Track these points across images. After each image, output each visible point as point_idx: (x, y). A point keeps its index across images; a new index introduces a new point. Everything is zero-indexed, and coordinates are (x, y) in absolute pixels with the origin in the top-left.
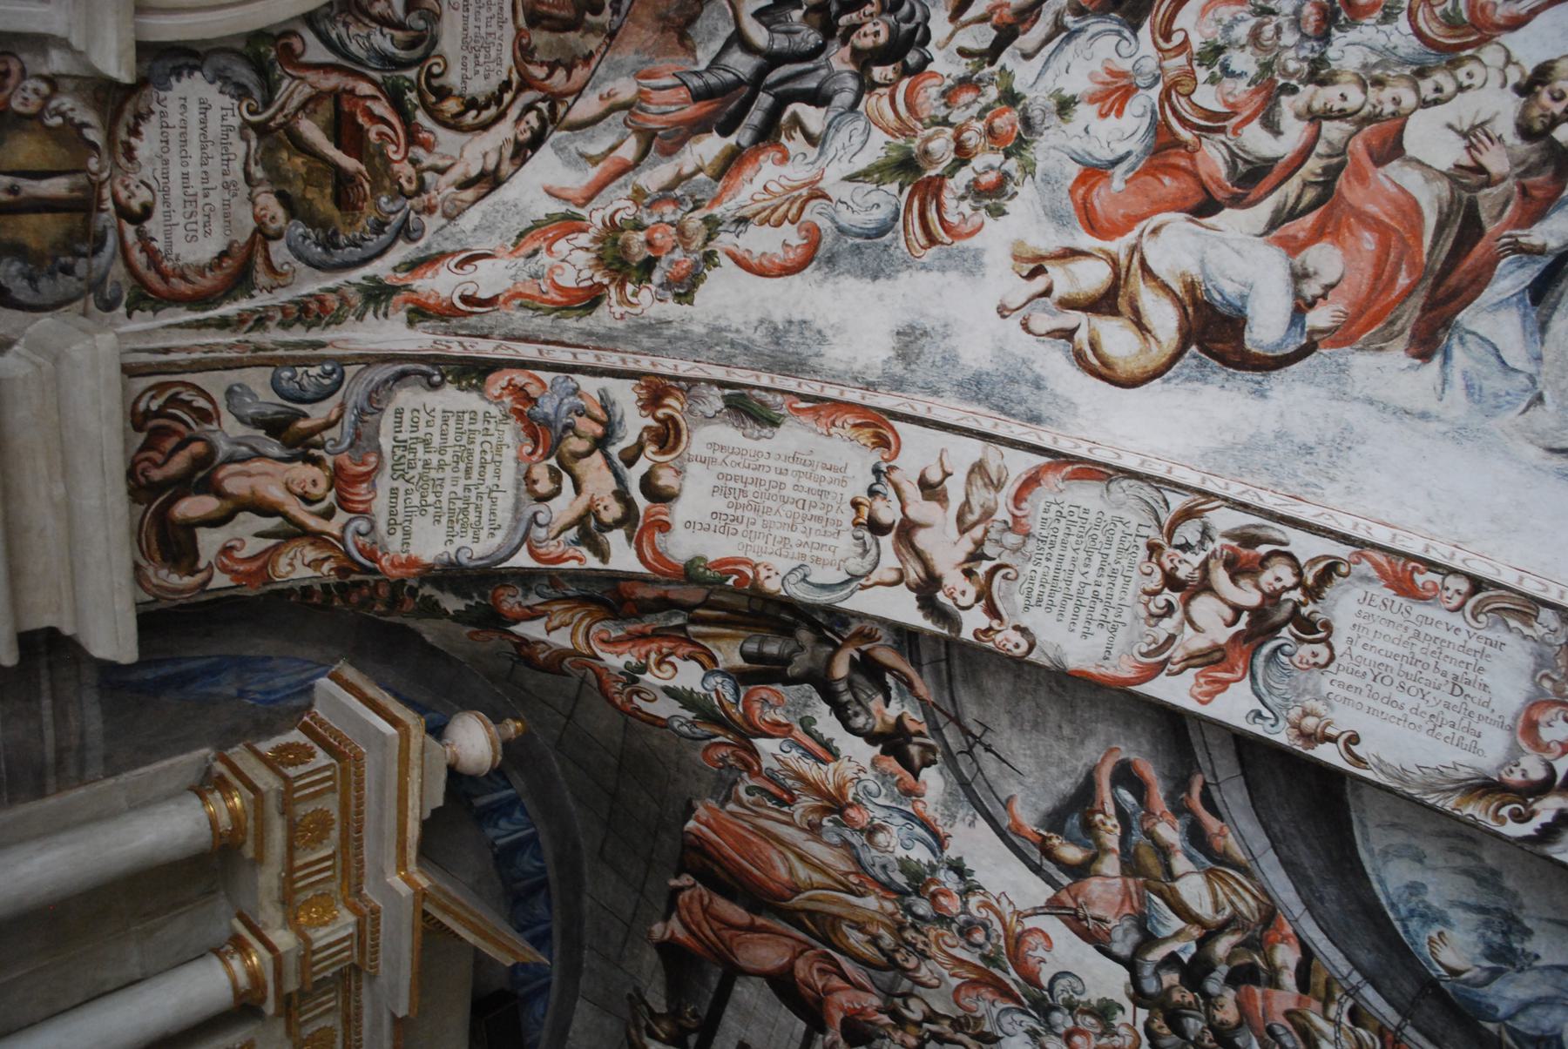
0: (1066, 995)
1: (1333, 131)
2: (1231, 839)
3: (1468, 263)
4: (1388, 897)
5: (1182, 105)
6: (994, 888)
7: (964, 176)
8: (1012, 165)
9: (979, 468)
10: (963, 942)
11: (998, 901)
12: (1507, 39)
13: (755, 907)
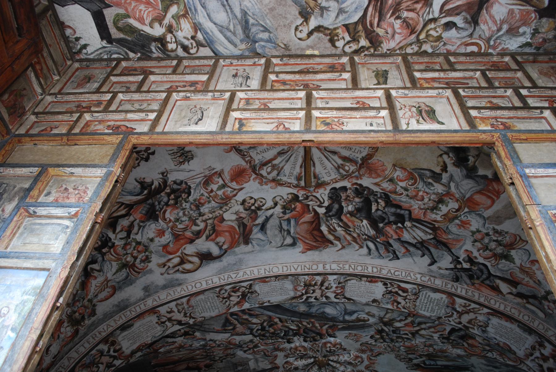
1: (209, 222)
3: (247, 230)
5: (176, 229)
7: (138, 260)
8: (147, 253)
9: (177, 305)
12: (234, 198)
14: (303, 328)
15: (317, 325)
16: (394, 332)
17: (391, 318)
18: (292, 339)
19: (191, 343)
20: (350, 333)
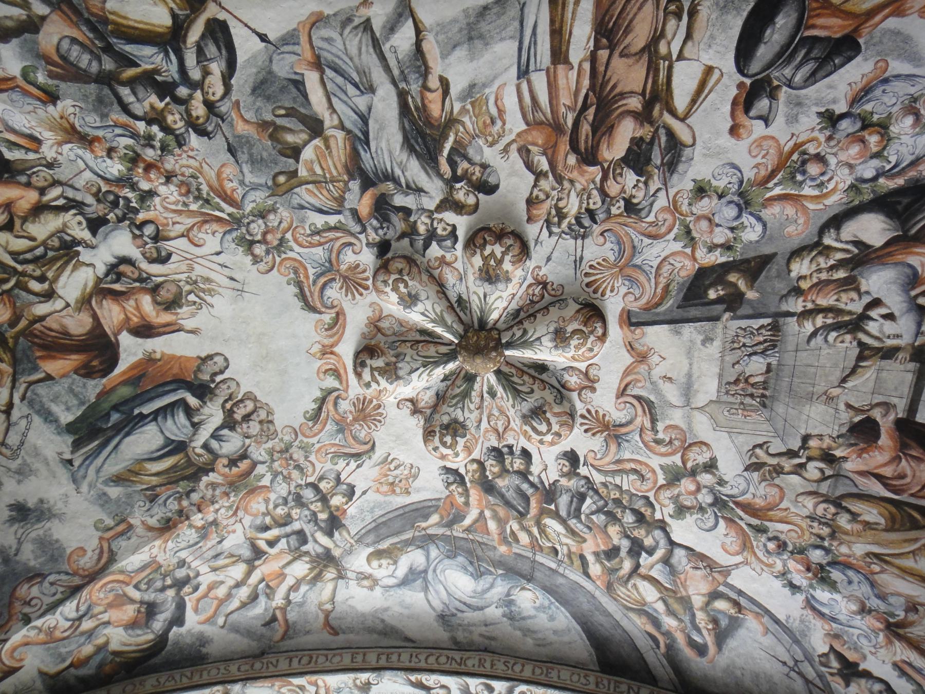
0: (706, 516)
10: (782, 537)
11: (762, 569)
14: (529, 522)
15: (492, 525)
16: (302, 536)
17: (319, 584)
18: (563, 475)
19: (858, 621)
20: (408, 493)
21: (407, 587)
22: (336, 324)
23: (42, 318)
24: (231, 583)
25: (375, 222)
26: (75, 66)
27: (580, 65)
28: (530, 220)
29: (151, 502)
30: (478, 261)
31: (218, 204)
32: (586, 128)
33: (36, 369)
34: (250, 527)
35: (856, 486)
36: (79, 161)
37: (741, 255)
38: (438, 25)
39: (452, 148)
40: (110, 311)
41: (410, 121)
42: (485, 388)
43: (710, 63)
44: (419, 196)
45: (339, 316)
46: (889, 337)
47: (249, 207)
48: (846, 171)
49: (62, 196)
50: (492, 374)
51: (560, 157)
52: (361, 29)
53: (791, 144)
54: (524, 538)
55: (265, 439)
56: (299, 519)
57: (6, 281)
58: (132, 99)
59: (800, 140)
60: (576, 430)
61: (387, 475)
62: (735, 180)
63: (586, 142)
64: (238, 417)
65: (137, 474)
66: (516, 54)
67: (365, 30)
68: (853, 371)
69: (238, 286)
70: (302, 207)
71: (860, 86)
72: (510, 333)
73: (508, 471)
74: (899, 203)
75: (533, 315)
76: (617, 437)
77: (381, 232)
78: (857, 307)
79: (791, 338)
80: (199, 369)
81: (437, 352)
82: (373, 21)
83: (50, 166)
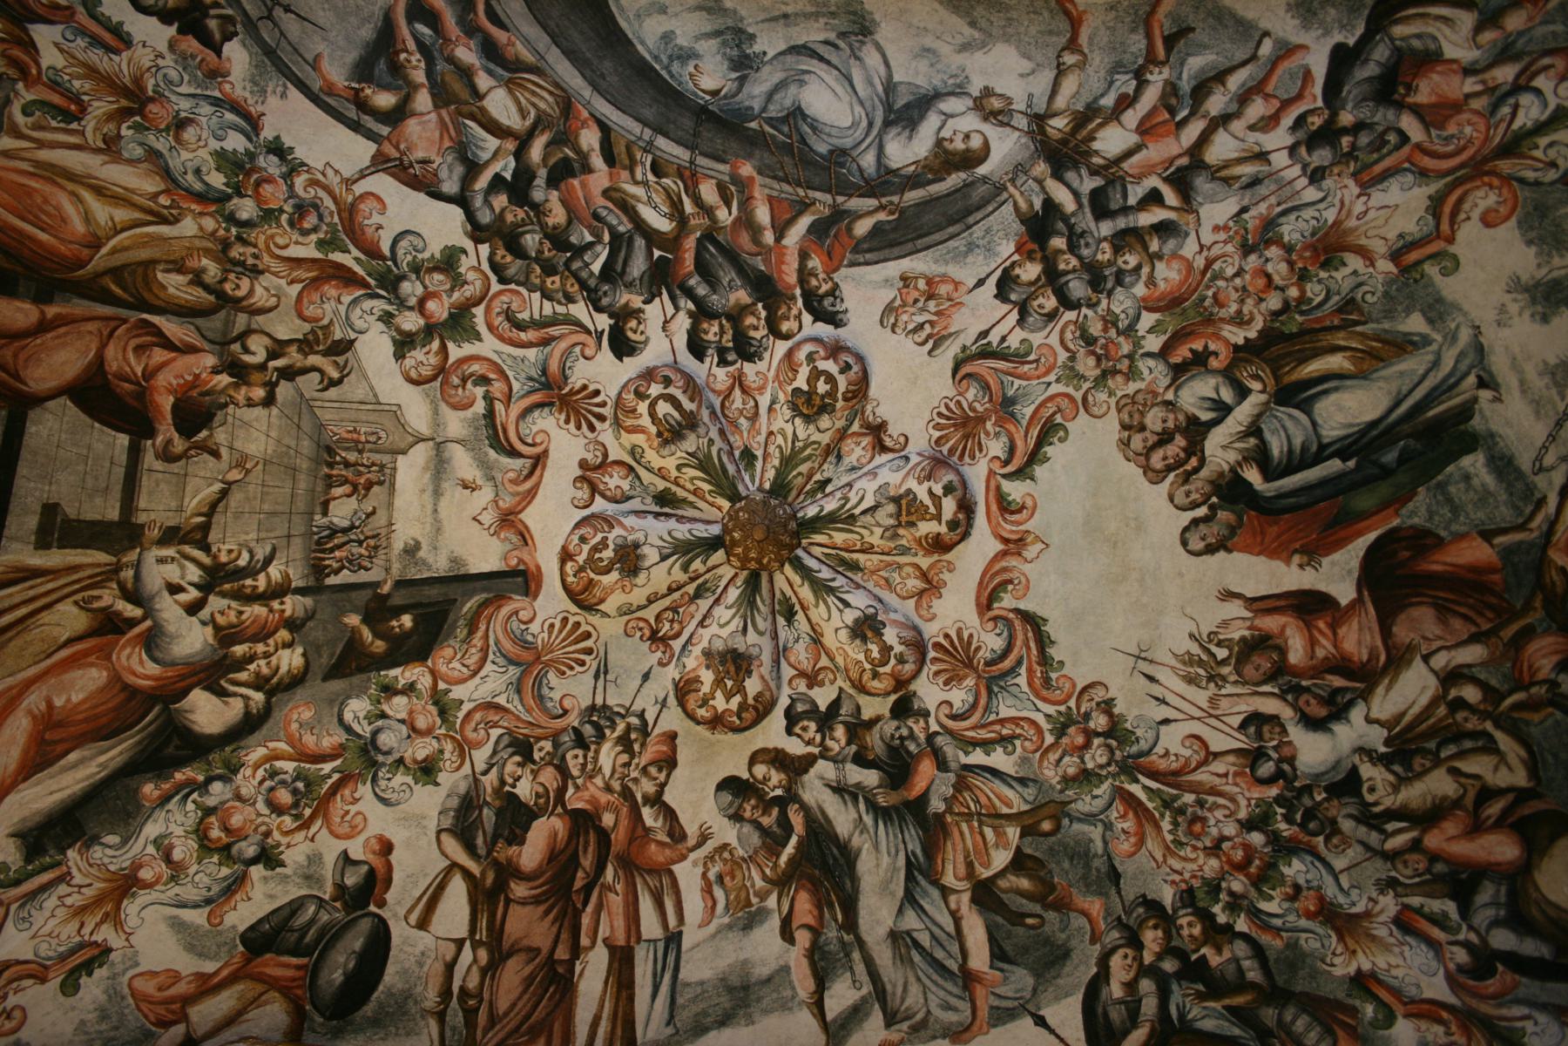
0: (409, 258)
2: (519, 46)
4: (650, 53)
6: (316, 162)
11: (324, 174)
13: (42, 297)
14: (698, 222)
15: (763, 214)
16: (1100, 206)
17: (1080, 107)
18: (636, 314)
20: (904, 278)
21: (923, 91)
22: (994, 590)
23: (1474, 639)
24: (1237, 126)
25: (912, 747)
26: (1316, 1019)
27: (594, 943)
28: (672, 736)
29: (1353, 300)
30: (753, 686)
31: (1150, 799)
32: (587, 861)
33: (1507, 553)
34: (1187, 234)
35: (198, 329)
36: (1345, 885)
37: (369, 679)
38: (790, 1009)
39: (784, 846)
40: (1359, 642)
41: (843, 889)
42: (759, 465)
43: (422, 933)
44: (839, 782)
45: (986, 602)
46: (173, 559)
47: (1104, 789)
48: (244, 791)
49: (1388, 835)
50: (744, 493)
51: (624, 823)
52: (899, 1016)
53: (313, 829)
54: (708, 192)
55: (1140, 398)
56: (1100, 241)
57: (1517, 706)
58: (1246, 964)
59: (303, 833)
60: (613, 393)
61: (938, 313)
62: (383, 783)
63: (587, 843)
64: (1180, 441)
65: (1371, 354)
66: (682, 964)
67: (895, 1013)
68: (213, 506)
69: (1143, 666)
70: (1023, 781)
71: (238, 897)
72: (710, 563)
73: (729, 317)
74: (177, 748)
75: (671, 590)
76: (547, 386)
77: (905, 732)
78: (215, 603)
79: (298, 556)
80: (1233, 530)
81: (831, 537)
82: (882, 1023)
83: (1391, 884)
